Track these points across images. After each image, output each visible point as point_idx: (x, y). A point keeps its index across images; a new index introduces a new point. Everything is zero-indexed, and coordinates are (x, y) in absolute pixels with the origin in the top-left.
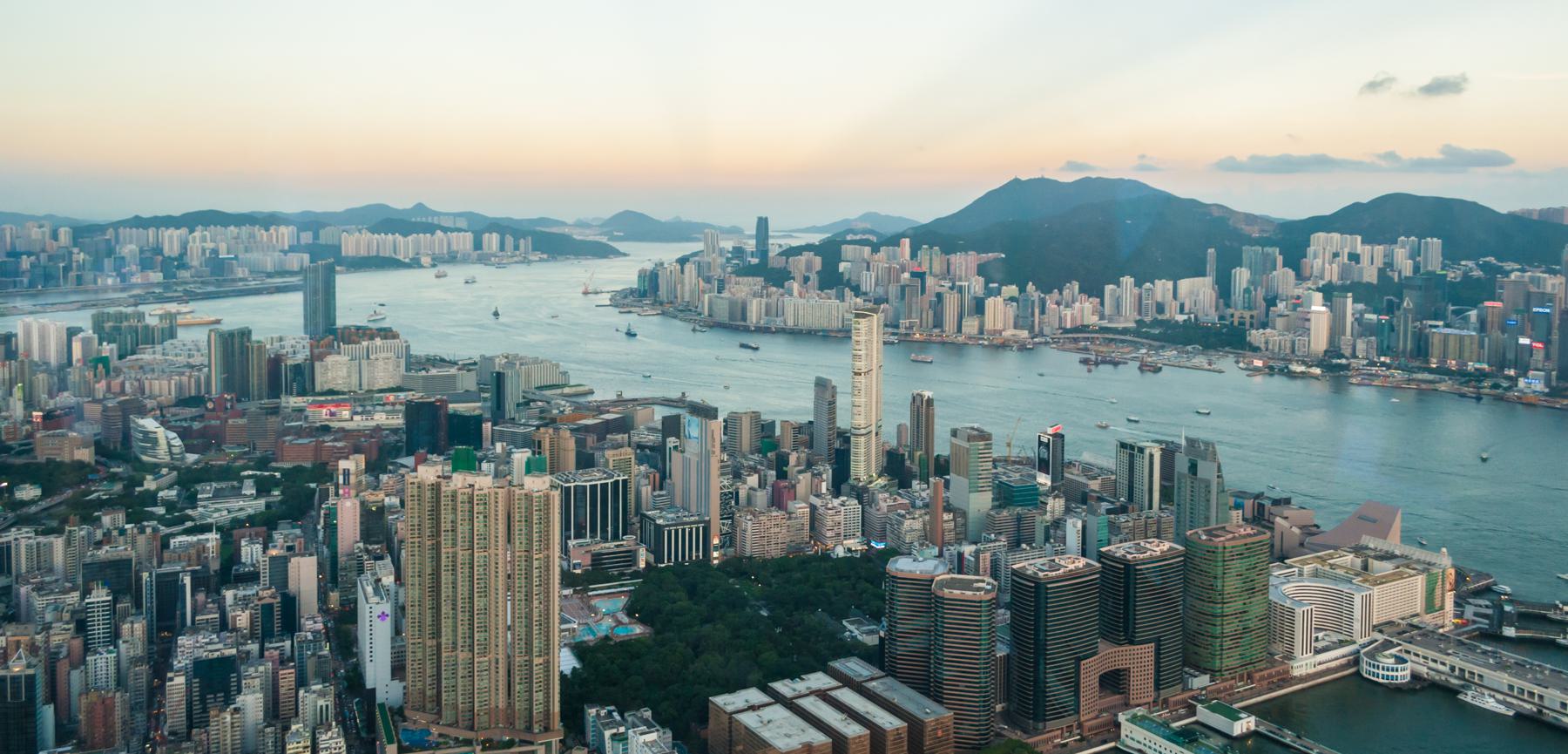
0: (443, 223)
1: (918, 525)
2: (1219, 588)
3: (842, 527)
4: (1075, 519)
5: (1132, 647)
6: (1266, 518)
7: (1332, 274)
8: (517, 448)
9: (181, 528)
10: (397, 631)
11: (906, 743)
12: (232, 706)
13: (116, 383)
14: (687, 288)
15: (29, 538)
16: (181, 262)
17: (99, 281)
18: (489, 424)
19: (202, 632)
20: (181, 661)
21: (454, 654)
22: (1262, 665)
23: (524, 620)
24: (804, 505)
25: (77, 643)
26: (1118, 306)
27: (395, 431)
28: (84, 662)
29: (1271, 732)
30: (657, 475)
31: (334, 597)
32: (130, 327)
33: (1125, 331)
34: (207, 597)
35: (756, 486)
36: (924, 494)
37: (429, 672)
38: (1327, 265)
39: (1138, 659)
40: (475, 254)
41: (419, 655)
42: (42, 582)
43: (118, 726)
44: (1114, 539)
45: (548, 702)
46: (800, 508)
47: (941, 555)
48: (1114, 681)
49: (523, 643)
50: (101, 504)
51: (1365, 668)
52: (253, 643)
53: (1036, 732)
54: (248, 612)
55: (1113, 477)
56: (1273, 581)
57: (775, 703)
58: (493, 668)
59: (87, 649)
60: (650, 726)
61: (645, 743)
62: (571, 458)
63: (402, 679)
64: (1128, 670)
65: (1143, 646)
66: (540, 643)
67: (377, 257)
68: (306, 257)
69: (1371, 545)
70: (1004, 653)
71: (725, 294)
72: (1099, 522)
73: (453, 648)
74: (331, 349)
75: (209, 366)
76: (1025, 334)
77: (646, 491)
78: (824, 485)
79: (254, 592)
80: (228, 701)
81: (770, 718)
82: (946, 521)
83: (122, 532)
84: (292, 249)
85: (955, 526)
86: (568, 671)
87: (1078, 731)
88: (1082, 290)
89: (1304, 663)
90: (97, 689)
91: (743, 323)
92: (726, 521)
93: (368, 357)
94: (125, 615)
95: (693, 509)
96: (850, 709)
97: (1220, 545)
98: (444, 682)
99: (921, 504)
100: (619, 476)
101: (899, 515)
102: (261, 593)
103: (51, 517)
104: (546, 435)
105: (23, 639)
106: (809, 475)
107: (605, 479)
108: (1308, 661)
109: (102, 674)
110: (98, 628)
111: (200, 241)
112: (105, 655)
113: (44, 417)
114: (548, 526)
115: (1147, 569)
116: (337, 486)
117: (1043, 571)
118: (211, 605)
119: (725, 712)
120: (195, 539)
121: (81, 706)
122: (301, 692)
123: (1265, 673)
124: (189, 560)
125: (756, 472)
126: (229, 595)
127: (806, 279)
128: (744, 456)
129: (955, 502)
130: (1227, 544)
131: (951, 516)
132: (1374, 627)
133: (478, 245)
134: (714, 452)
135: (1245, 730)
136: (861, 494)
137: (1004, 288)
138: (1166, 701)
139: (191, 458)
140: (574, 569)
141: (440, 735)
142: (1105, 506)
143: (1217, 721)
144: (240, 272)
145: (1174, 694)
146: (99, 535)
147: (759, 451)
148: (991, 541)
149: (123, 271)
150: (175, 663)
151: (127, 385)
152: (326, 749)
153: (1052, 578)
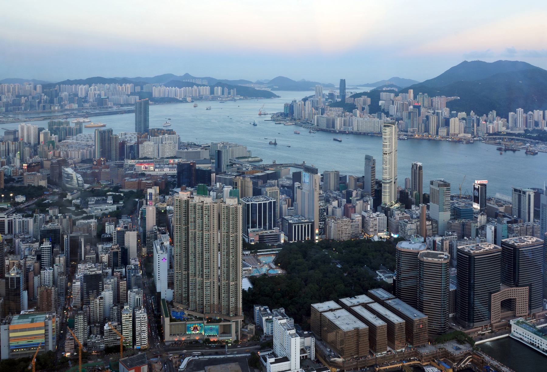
0: (197, 83)
1: (414, 226)
3: (377, 227)
8: (226, 185)
9: (81, 217)
10: (171, 267)
11: (404, 330)
12: (100, 296)
13: (57, 152)
14: (307, 112)
15: (20, 218)
16: (85, 100)
17: (52, 108)
18: (214, 174)
19: (88, 263)
20: (79, 275)
21: (195, 278)
24: (359, 216)
25: (37, 265)
27: (173, 176)
28: (40, 273)
30: (290, 200)
31: (144, 250)
32: (64, 128)
33: (519, 135)
34: (91, 248)
35: (337, 206)
36: (417, 212)
37: (184, 286)
40: (211, 96)
41: (180, 278)
42: (24, 238)
43: (53, 302)
44: (510, 236)
45: (237, 302)
47: (425, 241)
50: (49, 205)
52: (109, 269)
54: (107, 255)
55: (511, 206)
58: (212, 285)
59: (41, 268)
60: (283, 316)
62: (250, 191)
63: (172, 289)
66: (233, 275)
67: (168, 97)
68: (137, 97)
70: (454, 289)
71: (325, 116)
73: (194, 275)
75: (95, 146)
76: (469, 136)
77: (285, 207)
78: (369, 206)
79: (110, 246)
80: (98, 294)
81: (340, 315)
82: (428, 225)
83: (57, 217)
84: (132, 94)
86: (246, 289)
87: (490, 328)
88: (498, 115)
90: (44, 285)
91: (332, 129)
92: (322, 222)
94: (57, 253)
95: (306, 216)
96: (377, 312)
98: (190, 291)
99: (416, 217)
100: (272, 199)
101: (405, 221)
102: (113, 247)
103: (29, 210)
104: (239, 180)
105: (15, 262)
106: (362, 201)
107: (265, 201)
109: (47, 279)
110: (46, 259)
113: (28, 167)
114: (237, 222)
116: (147, 200)
118: (92, 251)
119: (319, 312)
120: (86, 221)
121: (38, 291)
122: (129, 292)
124: (84, 231)
125: (336, 200)
126: (100, 246)
127: (363, 109)
128: (331, 192)
129: (432, 216)
131: (430, 223)
133: (212, 92)
134: (316, 190)
136: (387, 211)
137: (459, 113)
138: (534, 315)
139: (87, 186)
140: (251, 242)
141: (189, 315)
144: (110, 104)
146: (48, 218)
148: (450, 235)
149: (62, 103)
150: (77, 276)
151: (61, 153)
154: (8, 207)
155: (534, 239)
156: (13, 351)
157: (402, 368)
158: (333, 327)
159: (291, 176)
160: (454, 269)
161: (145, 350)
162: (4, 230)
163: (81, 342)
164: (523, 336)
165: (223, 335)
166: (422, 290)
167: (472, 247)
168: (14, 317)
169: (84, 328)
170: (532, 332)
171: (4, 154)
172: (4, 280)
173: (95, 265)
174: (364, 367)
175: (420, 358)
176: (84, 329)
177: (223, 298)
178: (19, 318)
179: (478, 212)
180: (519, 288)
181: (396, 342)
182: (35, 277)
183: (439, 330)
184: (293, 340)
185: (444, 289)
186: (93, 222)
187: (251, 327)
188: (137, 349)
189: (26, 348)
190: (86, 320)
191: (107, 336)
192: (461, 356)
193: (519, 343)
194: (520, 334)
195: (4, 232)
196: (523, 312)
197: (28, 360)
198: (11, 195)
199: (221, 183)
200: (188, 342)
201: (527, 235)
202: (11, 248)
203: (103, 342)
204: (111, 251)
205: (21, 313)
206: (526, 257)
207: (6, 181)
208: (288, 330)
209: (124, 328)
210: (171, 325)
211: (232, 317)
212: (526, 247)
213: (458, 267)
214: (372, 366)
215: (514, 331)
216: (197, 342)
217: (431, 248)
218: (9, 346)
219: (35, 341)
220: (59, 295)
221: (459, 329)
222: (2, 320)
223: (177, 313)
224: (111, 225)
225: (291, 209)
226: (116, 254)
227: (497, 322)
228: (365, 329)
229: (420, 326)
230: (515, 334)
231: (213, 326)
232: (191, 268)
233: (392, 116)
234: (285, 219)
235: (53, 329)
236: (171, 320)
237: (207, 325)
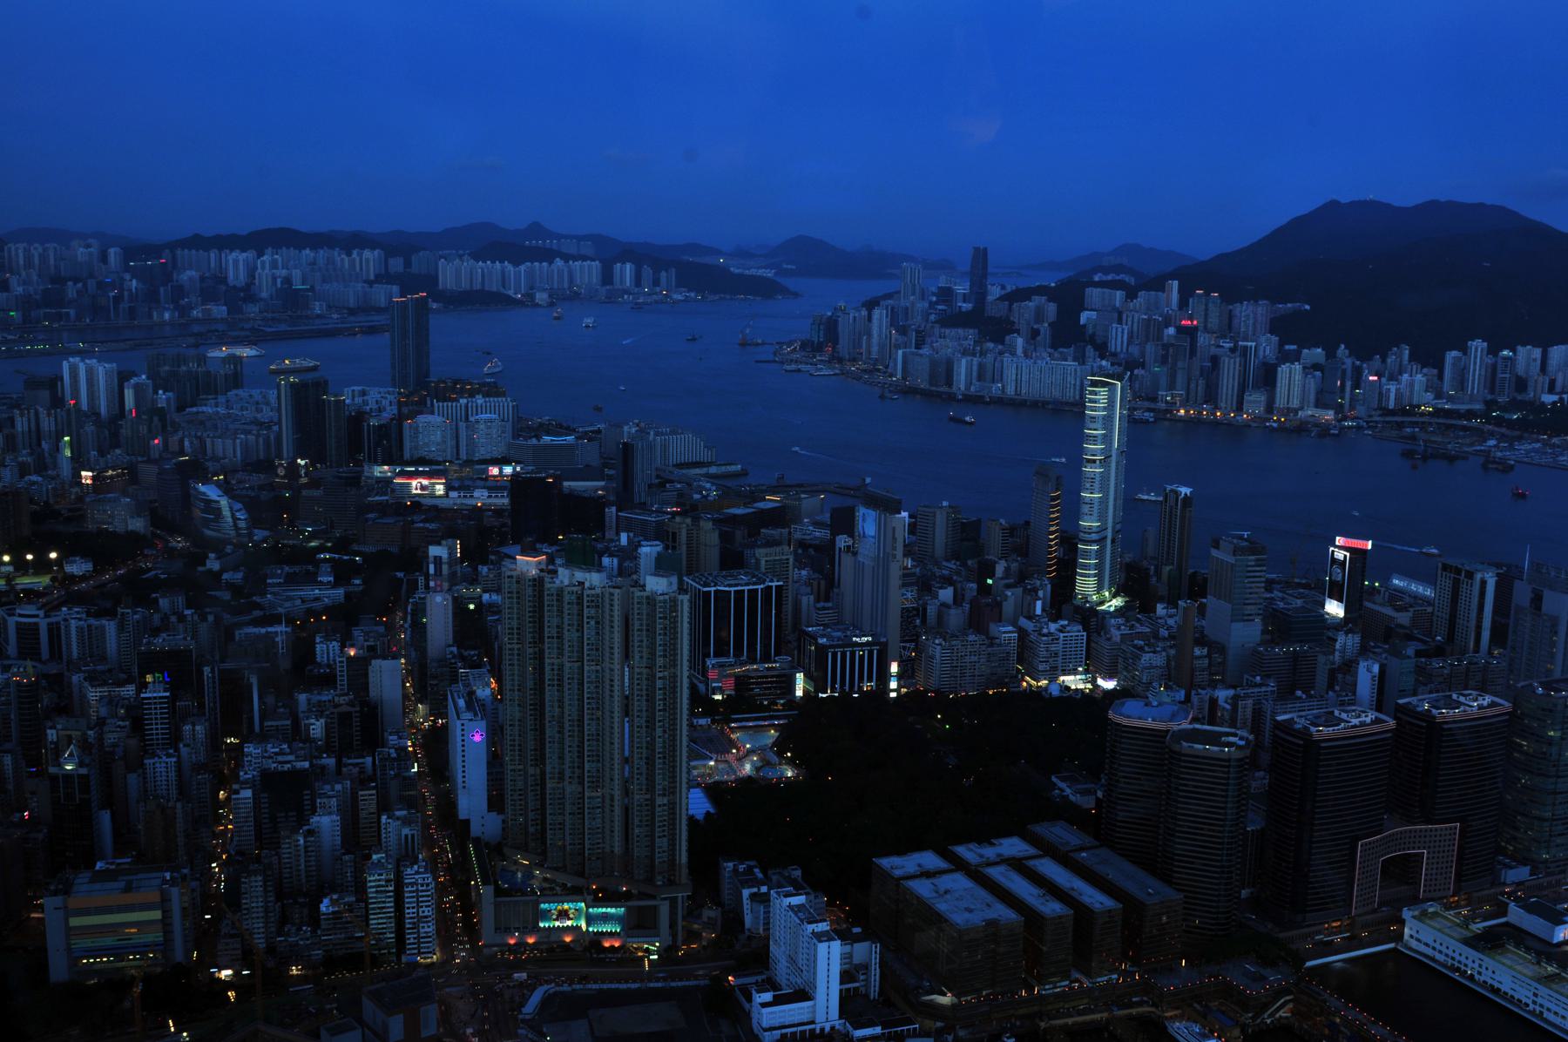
1: (1159, 660)
3: (1060, 659)
8: (646, 540)
9: (247, 618)
12: (305, 828)
15: (80, 619)
16: (247, 293)
18: (614, 509)
21: (561, 785)
23: (644, 751)
24: (1011, 628)
26: (1461, 383)
27: (499, 512)
28: (143, 764)
30: (823, 582)
33: (1470, 414)
36: (1171, 622)
41: (520, 785)
45: (674, 850)
46: (1006, 633)
47: (1188, 699)
48: (1402, 871)
49: (643, 778)
52: (328, 757)
54: (323, 721)
58: (607, 806)
61: (790, 906)
66: (664, 779)
68: (395, 289)
70: (1259, 827)
71: (925, 351)
73: (559, 778)
74: (421, 407)
75: (279, 423)
76: (1329, 415)
77: (807, 601)
78: (1039, 604)
79: (330, 697)
80: (302, 819)
81: (949, 887)
83: (182, 618)
84: (379, 279)
85: (1210, 663)
91: (944, 389)
92: (908, 645)
96: (1051, 883)
97: (1561, 701)
99: (1166, 634)
100: (772, 581)
101: (1135, 646)
102: (336, 699)
104: (683, 526)
105: (74, 734)
106: (1019, 591)
107: (754, 584)
110: (157, 728)
111: (270, 269)
113: (93, 478)
118: (282, 710)
119: (893, 878)
120: (263, 631)
122: (384, 818)
125: (951, 585)
127: (1035, 333)
131: (1205, 651)
133: (607, 278)
134: (894, 556)
136: (1090, 618)
139: (259, 534)
140: (714, 694)
141: (545, 879)
144: (318, 308)
146: (156, 618)
147: (955, 555)
148: (1256, 685)
149: (182, 302)
150: (242, 773)
151: (187, 443)
152: (412, 884)
155: (1487, 700)
159: (826, 517)
162: (40, 649)
163: (260, 942)
164: (1434, 948)
168: (81, 876)
173: (289, 747)
176: (266, 911)
178: (92, 881)
183: (1210, 930)
184: (822, 948)
190: (270, 889)
191: (330, 929)
194: (1427, 945)
195: (40, 654)
196: (1437, 888)
198: (53, 555)
199: (631, 535)
205: (97, 868)
206: (1460, 745)
208: (810, 923)
209: (374, 909)
210: (497, 905)
211: (659, 886)
215: (1412, 936)
217: (1204, 718)
223: (515, 873)
224: (331, 641)
225: (824, 608)
229: (1161, 919)
230: (1414, 944)
231: (609, 910)
232: (551, 752)
233: (1114, 355)
234: (807, 633)
235: (184, 908)
236: (499, 892)
237: (593, 907)
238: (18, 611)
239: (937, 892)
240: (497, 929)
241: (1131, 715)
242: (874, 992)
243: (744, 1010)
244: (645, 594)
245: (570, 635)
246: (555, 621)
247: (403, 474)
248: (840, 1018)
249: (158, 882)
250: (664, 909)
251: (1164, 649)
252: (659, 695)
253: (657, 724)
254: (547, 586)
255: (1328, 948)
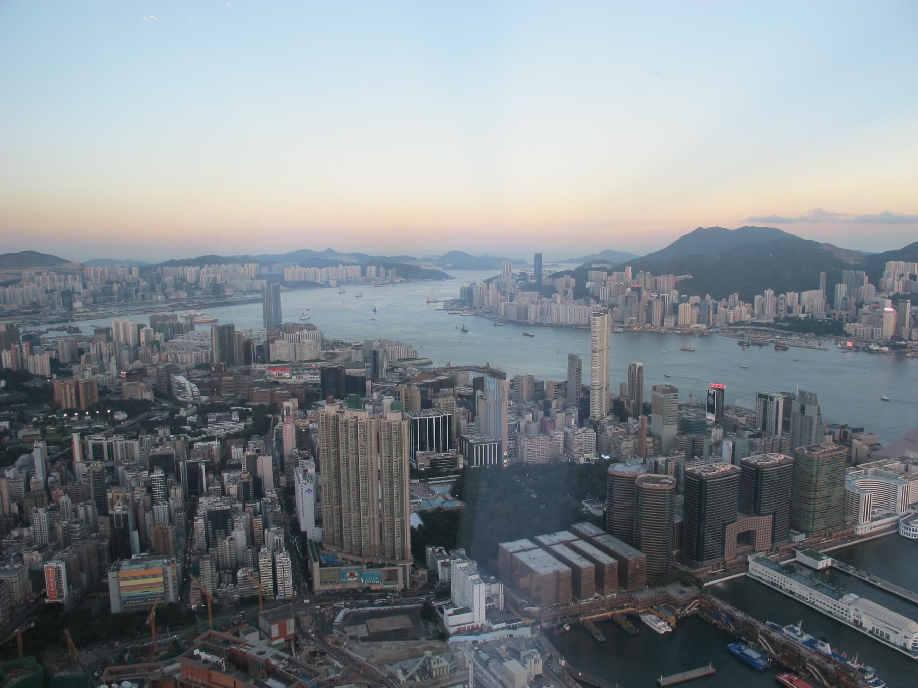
1: (630, 444)
2: (814, 482)
4: (728, 441)
5: (759, 517)
6: (848, 439)
7: (899, 287)
8: (386, 396)
9: (199, 438)
10: (318, 500)
11: (616, 572)
12: (229, 537)
14: (491, 299)
15: (122, 441)
16: (196, 286)
17: (154, 297)
20: (201, 511)
22: (839, 528)
23: (388, 496)
24: (560, 432)
25: (148, 498)
27: (315, 385)
28: (152, 509)
29: (841, 567)
30: (470, 413)
31: (283, 479)
33: (767, 325)
34: (214, 477)
35: (531, 421)
36: (635, 426)
38: (896, 282)
39: (762, 525)
41: (330, 514)
42: (129, 465)
44: (752, 453)
45: (404, 543)
47: (644, 462)
48: (746, 538)
50: (157, 423)
51: (902, 530)
53: (697, 567)
54: (236, 486)
56: (848, 478)
57: (539, 548)
58: (371, 522)
59: (153, 502)
60: (463, 558)
63: (321, 527)
64: (755, 531)
65: (765, 517)
66: (398, 509)
68: (265, 282)
69: (911, 456)
70: (680, 521)
71: (515, 302)
72: (743, 443)
75: (212, 346)
76: (703, 326)
77: (463, 422)
78: (573, 420)
80: (227, 533)
82: (648, 442)
83: (169, 439)
84: (258, 277)
87: (723, 566)
89: (864, 527)
92: (512, 442)
93: (299, 341)
94: (172, 484)
96: (583, 551)
97: (816, 456)
99: (633, 432)
100: (446, 413)
101: (619, 438)
102: (242, 475)
104: (403, 388)
105: (121, 495)
106: (563, 414)
107: (438, 415)
108: (867, 526)
109: (161, 516)
110: (158, 491)
112: (162, 506)
113: (127, 375)
115: (770, 471)
117: (705, 472)
118: (216, 481)
119: (508, 552)
120: (207, 444)
122: (266, 531)
123: (840, 533)
124: (204, 456)
126: (225, 476)
127: (566, 293)
129: (654, 431)
130: (820, 456)
131: (652, 439)
132: (909, 505)
133: (363, 273)
135: (824, 566)
136: (596, 426)
137: (691, 297)
138: (777, 549)
139: (204, 398)
141: (343, 559)
142: (748, 433)
143: (808, 560)
144: (229, 291)
145: (784, 545)
146: (157, 440)
147: (533, 399)
148: (676, 454)
149: (166, 291)
151: (169, 357)
153: (711, 476)
154: (105, 426)
155: (782, 457)
156: (125, 603)
157: (613, 618)
158: (527, 570)
160: (680, 496)
161: (289, 601)
162: (103, 455)
163: (209, 592)
165: (387, 582)
166: (639, 523)
167: (705, 468)
169: (212, 575)
170: (774, 570)
171: (96, 358)
172: (108, 518)
174: (565, 617)
175: (635, 605)
176: (212, 577)
177: (386, 538)
178: (131, 564)
179: (713, 424)
180: (761, 517)
181: (606, 587)
182: (146, 514)
184: (476, 587)
185: (667, 521)
186: (215, 444)
187: (423, 572)
188: (279, 600)
189: (142, 599)
191: (241, 585)
192: (686, 601)
193: (758, 584)
194: (760, 573)
195: (103, 457)
197: (144, 614)
198: (109, 411)
199: (379, 394)
200: (344, 591)
201: (772, 452)
202: (113, 478)
203: (237, 592)
204: (240, 480)
207: (101, 394)
208: (470, 575)
210: (321, 571)
212: (771, 467)
213: (684, 494)
214: (576, 616)
216: (354, 591)
218: (120, 597)
219: (152, 591)
220: (177, 535)
221: (685, 568)
222: (109, 566)
225: (471, 426)
226: (246, 485)
227: (732, 559)
228: (567, 572)
230: (754, 573)
231: (374, 572)
233: (603, 301)
235: (174, 576)
236: (321, 565)
238: (93, 438)
239: (530, 558)
240: (321, 583)
241: (618, 469)
242: (501, 607)
243: (439, 617)
244: (386, 422)
245: (351, 442)
246: (344, 436)
247: (269, 368)
248: (486, 619)
249: (161, 564)
250: (400, 571)
251: (632, 439)
252: (394, 469)
253: (394, 483)
254: (340, 419)
255: (714, 576)
